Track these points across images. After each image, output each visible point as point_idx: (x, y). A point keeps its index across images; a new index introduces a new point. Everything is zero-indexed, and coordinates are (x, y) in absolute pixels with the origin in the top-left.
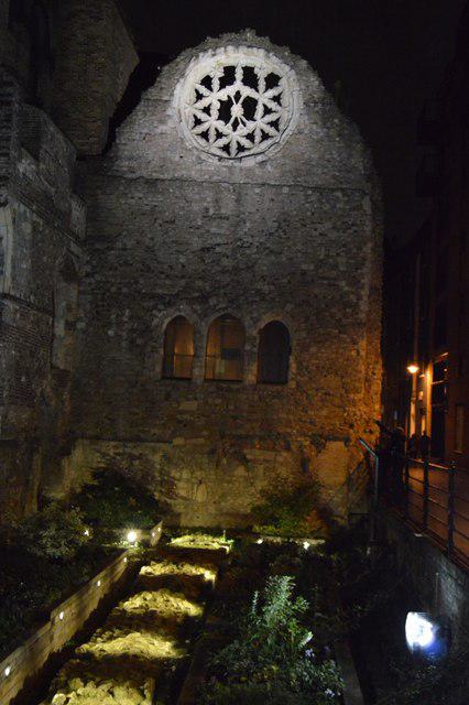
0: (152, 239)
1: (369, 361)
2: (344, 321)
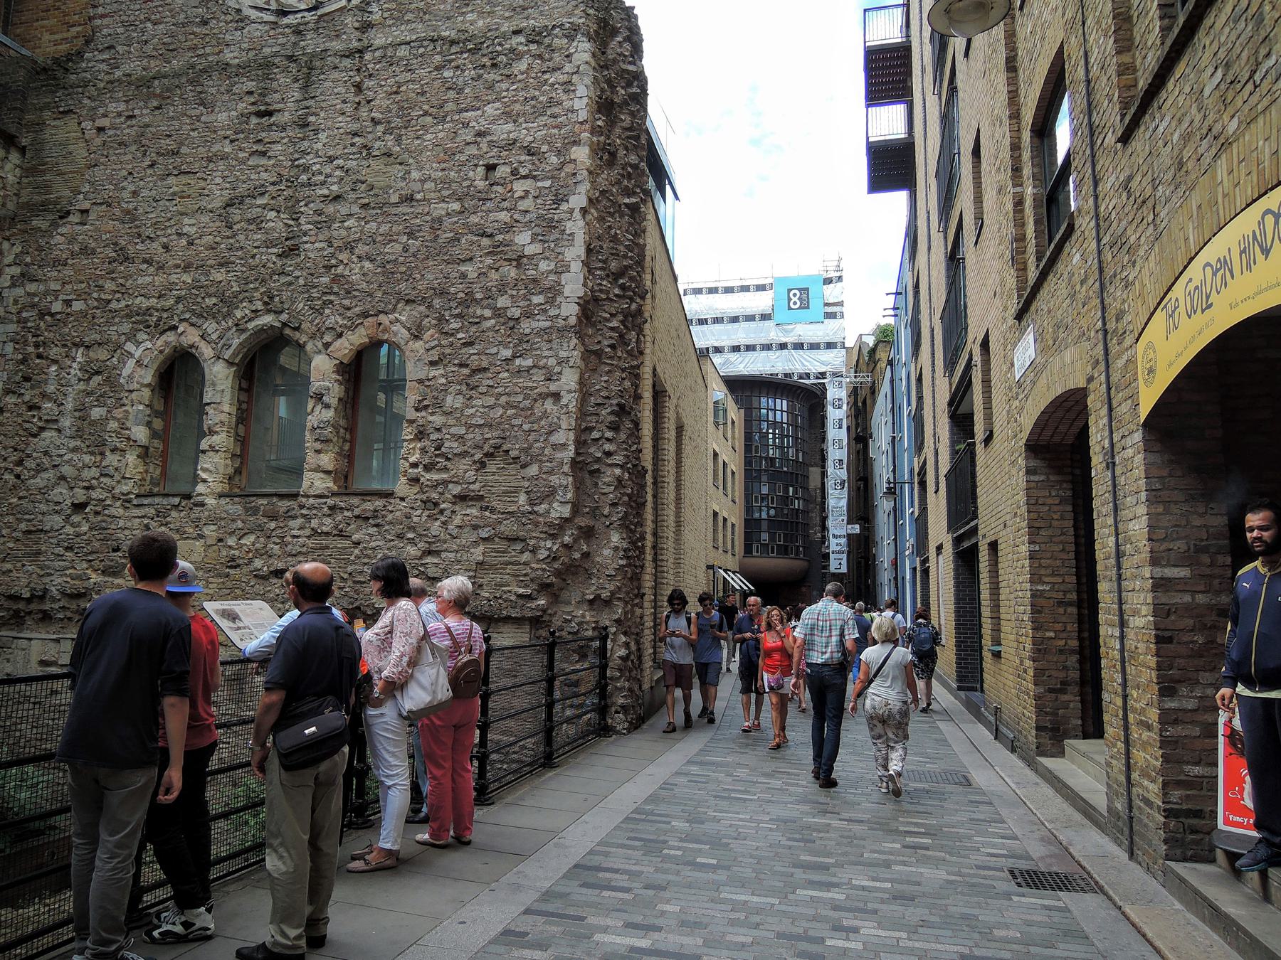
0: (135, 193)
1: (592, 421)
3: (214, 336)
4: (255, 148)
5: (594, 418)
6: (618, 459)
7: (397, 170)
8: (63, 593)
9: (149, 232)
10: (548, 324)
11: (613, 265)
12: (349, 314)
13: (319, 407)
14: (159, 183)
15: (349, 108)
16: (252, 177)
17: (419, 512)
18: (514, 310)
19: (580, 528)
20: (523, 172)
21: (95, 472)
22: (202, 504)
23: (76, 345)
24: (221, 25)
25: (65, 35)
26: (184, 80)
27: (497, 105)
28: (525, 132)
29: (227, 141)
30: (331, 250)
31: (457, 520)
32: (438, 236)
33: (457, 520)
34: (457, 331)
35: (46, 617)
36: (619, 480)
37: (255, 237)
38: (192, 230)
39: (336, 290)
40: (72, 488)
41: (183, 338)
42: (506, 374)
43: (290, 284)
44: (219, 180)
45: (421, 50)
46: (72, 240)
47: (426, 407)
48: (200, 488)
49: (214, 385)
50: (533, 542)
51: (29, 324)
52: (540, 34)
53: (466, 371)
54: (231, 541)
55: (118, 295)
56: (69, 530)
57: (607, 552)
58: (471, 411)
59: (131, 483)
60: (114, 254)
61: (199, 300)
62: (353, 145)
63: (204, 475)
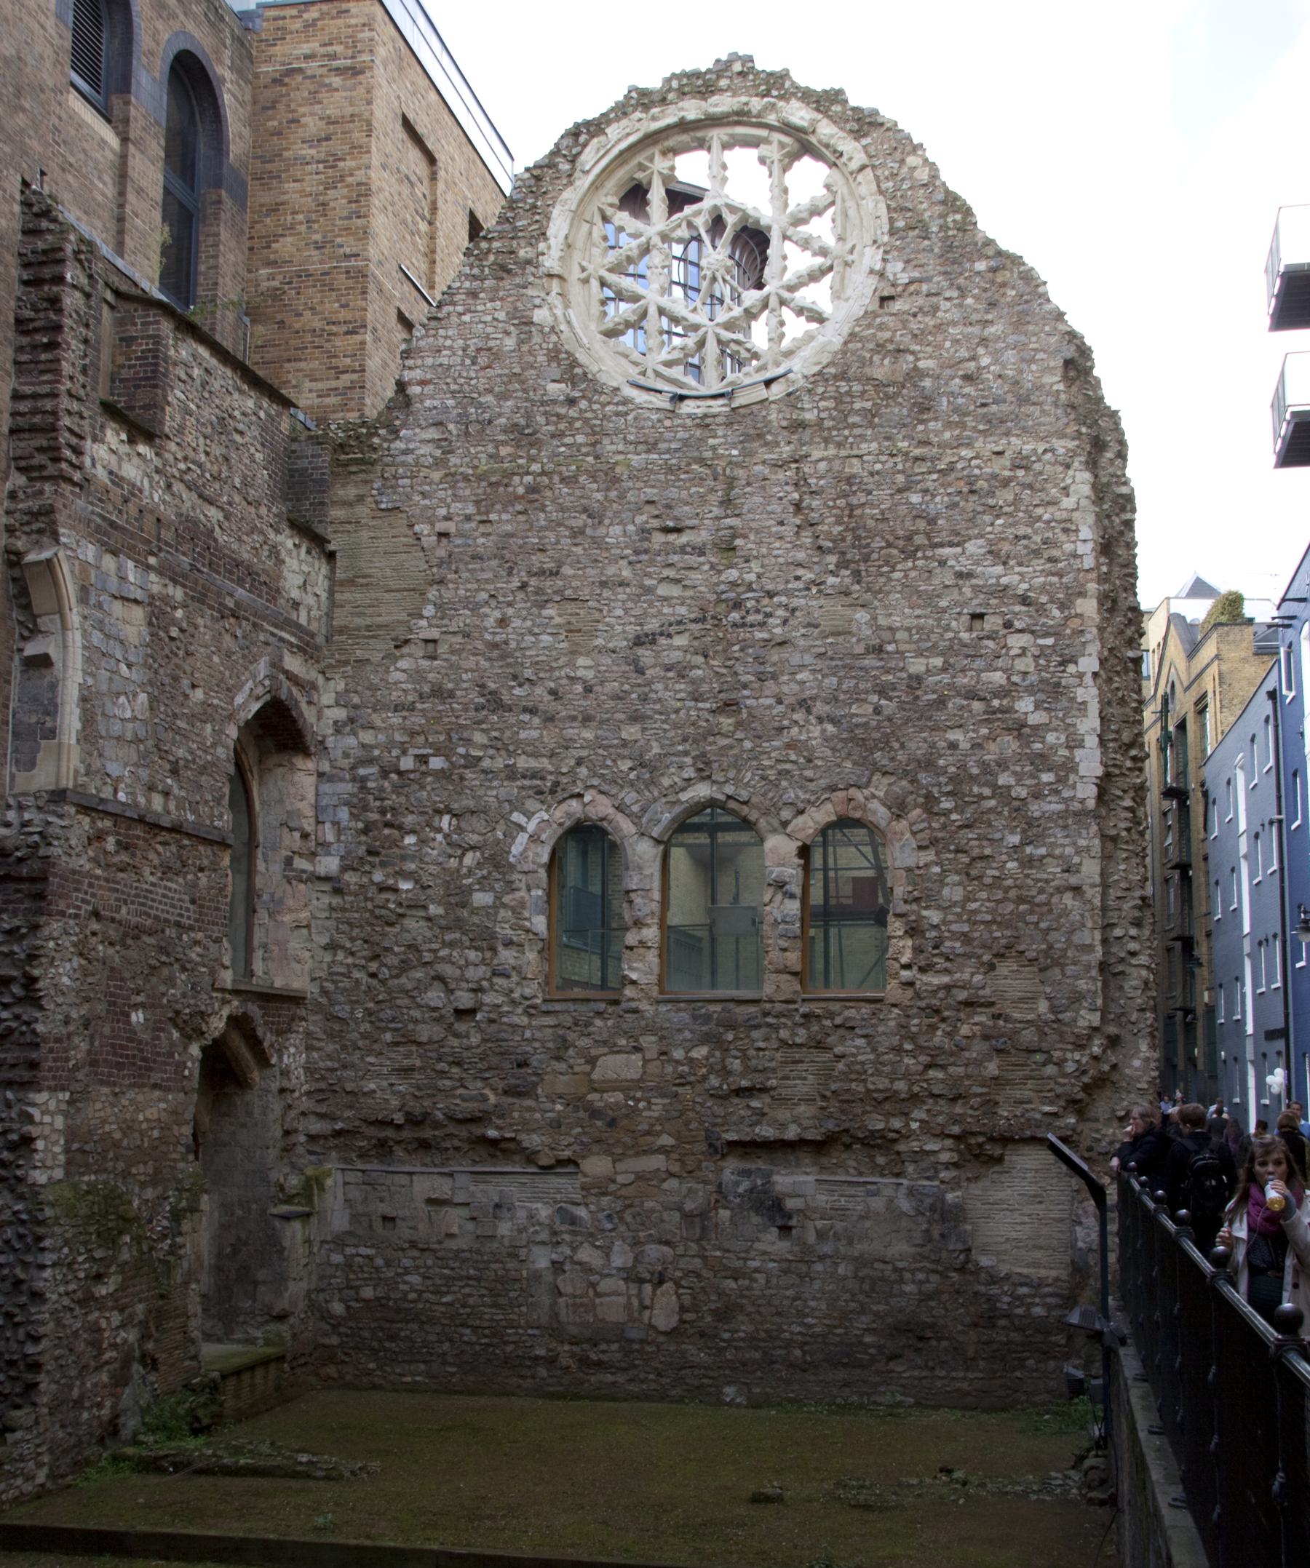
0: (503, 622)
2: (1035, 809)
3: (635, 808)
4: (666, 573)
5: (1116, 914)
6: (1143, 959)
7: (862, 616)
8: (451, 1118)
9: (528, 673)
10: (1061, 807)
11: (1126, 736)
12: (812, 786)
13: (779, 897)
14: (535, 610)
15: (788, 531)
16: (665, 610)
17: (916, 1021)
18: (1019, 789)
19: (1108, 1037)
20: (1018, 624)
21: (482, 971)
22: (636, 1011)
23: (439, 812)
24: (595, 407)
25: (333, 384)
26: (556, 479)
27: (980, 542)
28: (1017, 578)
29: (624, 563)
30: (781, 708)
31: (965, 1030)
32: (917, 698)
33: (965, 1030)
34: (950, 811)
35: (424, 1145)
36: (1146, 983)
37: (678, 687)
38: (589, 674)
39: (793, 757)
40: (452, 991)
41: (588, 808)
42: (1015, 864)
43: (731, 747)
44: (619, 612)
45: (878, 467)
46: (417, 675)
47: (917, 900)
48: (629, 992)
49: (640, 868)
50: (1057, 1054)
51: (371, 785)
52: (1027, 457)
53: (965, 859)
54: (678, 1054)
55: (491, 752)
56: (456, 1042)
57: (1137, 1063)
58: (974, 906)
59: (534, 985)
60: (482, 700)
61: (609, 762)
62: (798, 578)
63: (634, 976)
